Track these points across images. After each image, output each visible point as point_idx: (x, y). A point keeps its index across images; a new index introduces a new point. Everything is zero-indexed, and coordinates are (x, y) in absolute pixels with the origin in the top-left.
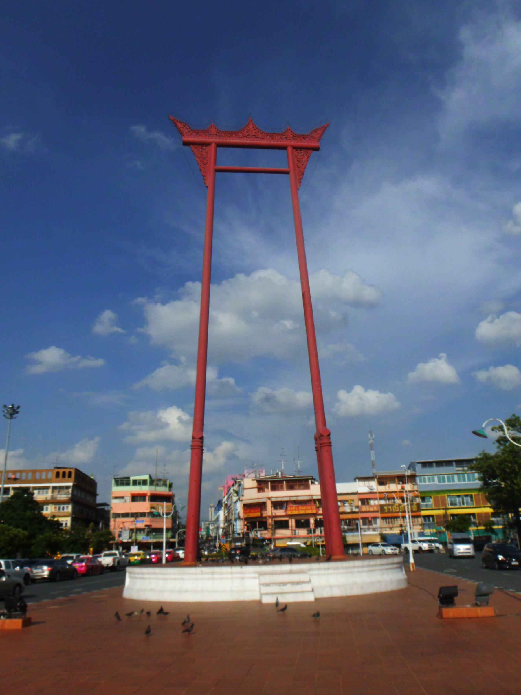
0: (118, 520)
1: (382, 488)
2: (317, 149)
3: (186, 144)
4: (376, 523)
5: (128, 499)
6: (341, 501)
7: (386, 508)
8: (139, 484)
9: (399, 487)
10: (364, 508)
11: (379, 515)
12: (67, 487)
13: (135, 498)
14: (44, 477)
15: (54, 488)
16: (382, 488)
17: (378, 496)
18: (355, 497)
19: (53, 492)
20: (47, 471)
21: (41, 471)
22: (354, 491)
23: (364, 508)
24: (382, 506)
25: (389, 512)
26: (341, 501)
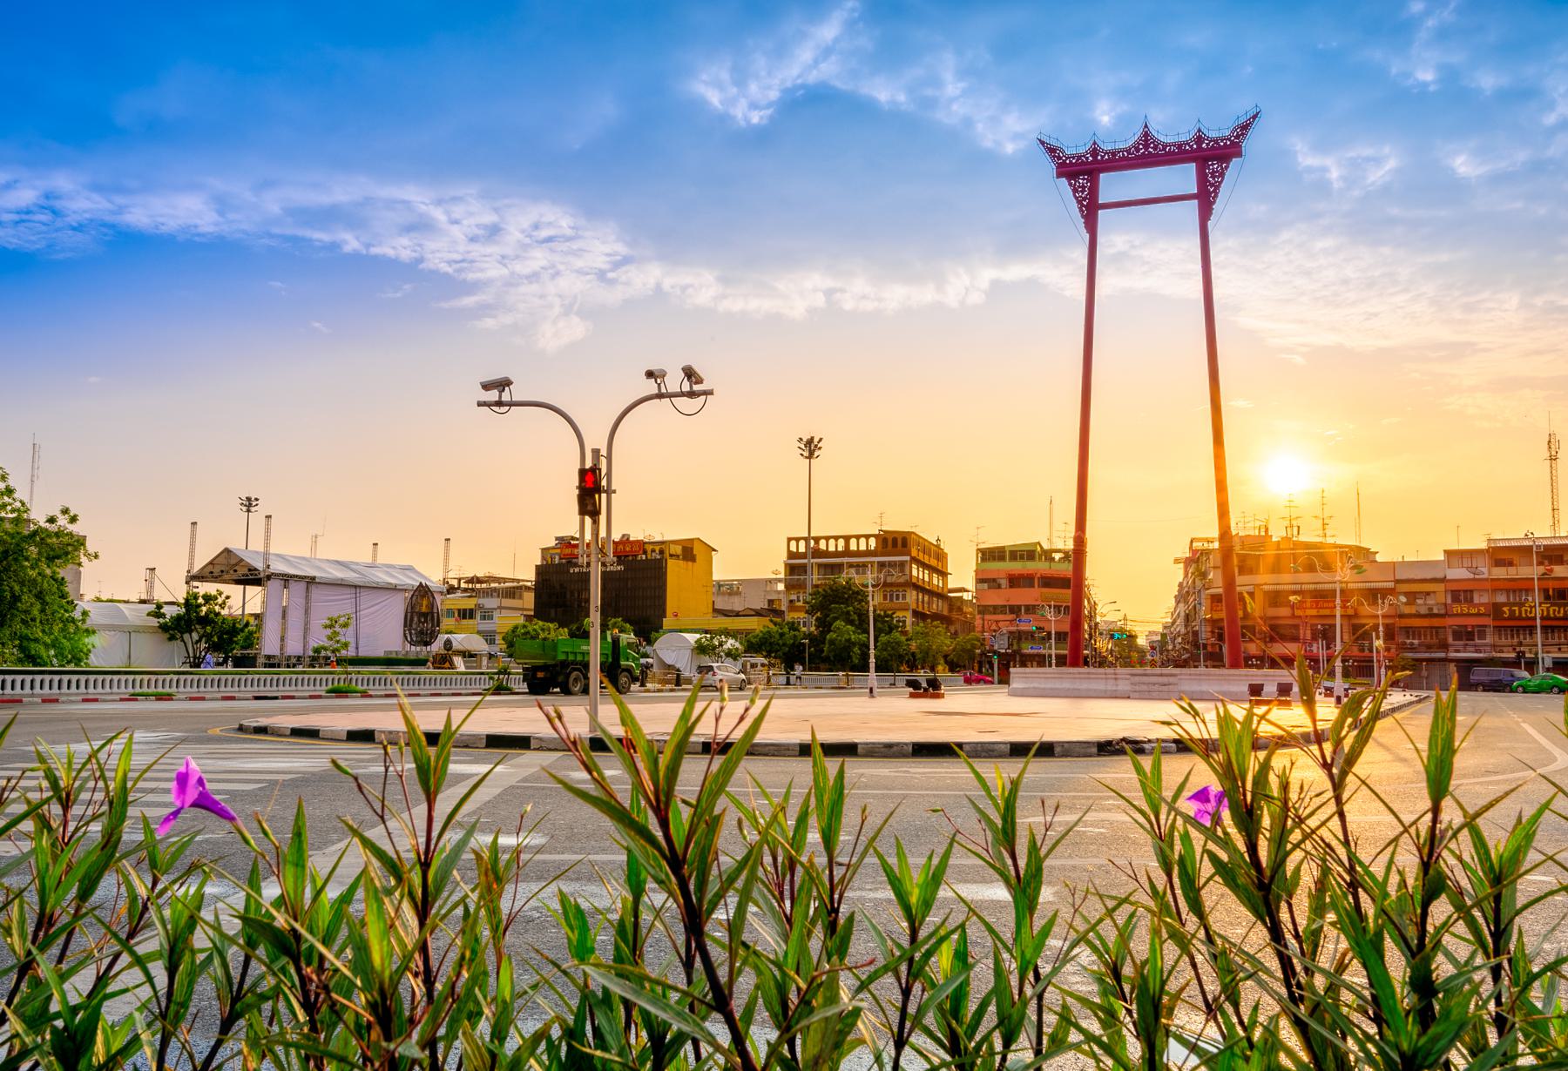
0: (987, 617)
1: (1501, 573)
2: (1239, 154)
3: (1059, 175)
4: (1482, 635)
5: (1004, 583)
6: (1406, 594)
7: (1506, 609)
8: (1022, 557)
9: (1542, 569)
10: (1457, 609)
11: (1488, 621)
12: (902, 564)
13: (1015, 581)
14: (863, 547)
15: (882, 565)
16: (1501, 573)
17: (1488, 585)
18: (1440, 587)
19: (880, 571)
20: (867, 537)
21: (858, 537)
22: (1440, 575)
23: (1457, 609)
24: (1497, 607)
25: (1512, 617)
26: (1406, 594)
